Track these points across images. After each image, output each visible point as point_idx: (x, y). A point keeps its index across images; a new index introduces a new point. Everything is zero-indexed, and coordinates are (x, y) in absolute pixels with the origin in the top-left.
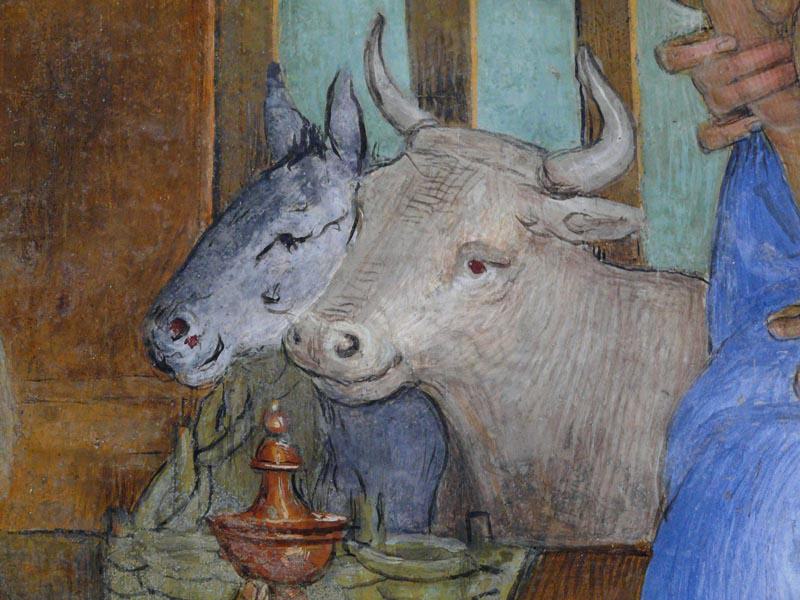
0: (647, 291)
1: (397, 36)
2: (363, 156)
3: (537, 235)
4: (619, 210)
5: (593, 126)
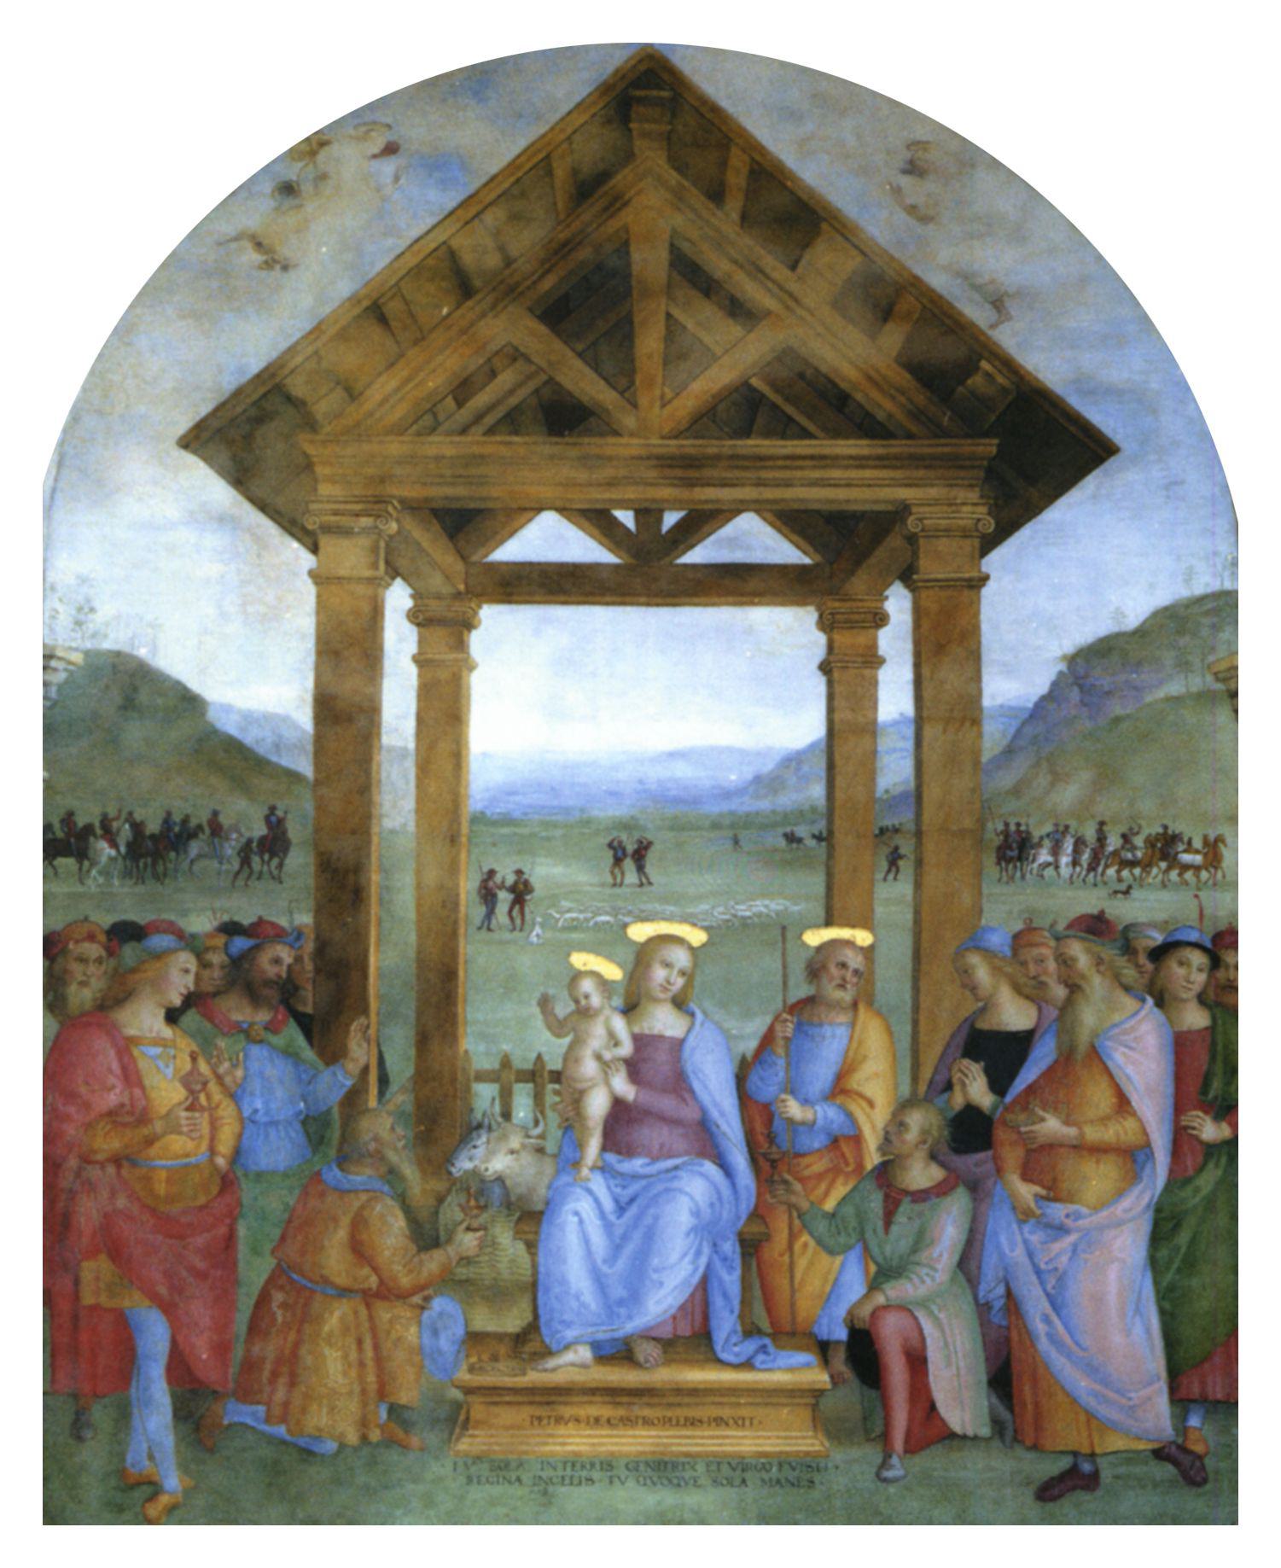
1: (497, 1102)
2: (490, 1129)
3: (524, 1146)
4: (539, 1141)
5: (536, 1123)
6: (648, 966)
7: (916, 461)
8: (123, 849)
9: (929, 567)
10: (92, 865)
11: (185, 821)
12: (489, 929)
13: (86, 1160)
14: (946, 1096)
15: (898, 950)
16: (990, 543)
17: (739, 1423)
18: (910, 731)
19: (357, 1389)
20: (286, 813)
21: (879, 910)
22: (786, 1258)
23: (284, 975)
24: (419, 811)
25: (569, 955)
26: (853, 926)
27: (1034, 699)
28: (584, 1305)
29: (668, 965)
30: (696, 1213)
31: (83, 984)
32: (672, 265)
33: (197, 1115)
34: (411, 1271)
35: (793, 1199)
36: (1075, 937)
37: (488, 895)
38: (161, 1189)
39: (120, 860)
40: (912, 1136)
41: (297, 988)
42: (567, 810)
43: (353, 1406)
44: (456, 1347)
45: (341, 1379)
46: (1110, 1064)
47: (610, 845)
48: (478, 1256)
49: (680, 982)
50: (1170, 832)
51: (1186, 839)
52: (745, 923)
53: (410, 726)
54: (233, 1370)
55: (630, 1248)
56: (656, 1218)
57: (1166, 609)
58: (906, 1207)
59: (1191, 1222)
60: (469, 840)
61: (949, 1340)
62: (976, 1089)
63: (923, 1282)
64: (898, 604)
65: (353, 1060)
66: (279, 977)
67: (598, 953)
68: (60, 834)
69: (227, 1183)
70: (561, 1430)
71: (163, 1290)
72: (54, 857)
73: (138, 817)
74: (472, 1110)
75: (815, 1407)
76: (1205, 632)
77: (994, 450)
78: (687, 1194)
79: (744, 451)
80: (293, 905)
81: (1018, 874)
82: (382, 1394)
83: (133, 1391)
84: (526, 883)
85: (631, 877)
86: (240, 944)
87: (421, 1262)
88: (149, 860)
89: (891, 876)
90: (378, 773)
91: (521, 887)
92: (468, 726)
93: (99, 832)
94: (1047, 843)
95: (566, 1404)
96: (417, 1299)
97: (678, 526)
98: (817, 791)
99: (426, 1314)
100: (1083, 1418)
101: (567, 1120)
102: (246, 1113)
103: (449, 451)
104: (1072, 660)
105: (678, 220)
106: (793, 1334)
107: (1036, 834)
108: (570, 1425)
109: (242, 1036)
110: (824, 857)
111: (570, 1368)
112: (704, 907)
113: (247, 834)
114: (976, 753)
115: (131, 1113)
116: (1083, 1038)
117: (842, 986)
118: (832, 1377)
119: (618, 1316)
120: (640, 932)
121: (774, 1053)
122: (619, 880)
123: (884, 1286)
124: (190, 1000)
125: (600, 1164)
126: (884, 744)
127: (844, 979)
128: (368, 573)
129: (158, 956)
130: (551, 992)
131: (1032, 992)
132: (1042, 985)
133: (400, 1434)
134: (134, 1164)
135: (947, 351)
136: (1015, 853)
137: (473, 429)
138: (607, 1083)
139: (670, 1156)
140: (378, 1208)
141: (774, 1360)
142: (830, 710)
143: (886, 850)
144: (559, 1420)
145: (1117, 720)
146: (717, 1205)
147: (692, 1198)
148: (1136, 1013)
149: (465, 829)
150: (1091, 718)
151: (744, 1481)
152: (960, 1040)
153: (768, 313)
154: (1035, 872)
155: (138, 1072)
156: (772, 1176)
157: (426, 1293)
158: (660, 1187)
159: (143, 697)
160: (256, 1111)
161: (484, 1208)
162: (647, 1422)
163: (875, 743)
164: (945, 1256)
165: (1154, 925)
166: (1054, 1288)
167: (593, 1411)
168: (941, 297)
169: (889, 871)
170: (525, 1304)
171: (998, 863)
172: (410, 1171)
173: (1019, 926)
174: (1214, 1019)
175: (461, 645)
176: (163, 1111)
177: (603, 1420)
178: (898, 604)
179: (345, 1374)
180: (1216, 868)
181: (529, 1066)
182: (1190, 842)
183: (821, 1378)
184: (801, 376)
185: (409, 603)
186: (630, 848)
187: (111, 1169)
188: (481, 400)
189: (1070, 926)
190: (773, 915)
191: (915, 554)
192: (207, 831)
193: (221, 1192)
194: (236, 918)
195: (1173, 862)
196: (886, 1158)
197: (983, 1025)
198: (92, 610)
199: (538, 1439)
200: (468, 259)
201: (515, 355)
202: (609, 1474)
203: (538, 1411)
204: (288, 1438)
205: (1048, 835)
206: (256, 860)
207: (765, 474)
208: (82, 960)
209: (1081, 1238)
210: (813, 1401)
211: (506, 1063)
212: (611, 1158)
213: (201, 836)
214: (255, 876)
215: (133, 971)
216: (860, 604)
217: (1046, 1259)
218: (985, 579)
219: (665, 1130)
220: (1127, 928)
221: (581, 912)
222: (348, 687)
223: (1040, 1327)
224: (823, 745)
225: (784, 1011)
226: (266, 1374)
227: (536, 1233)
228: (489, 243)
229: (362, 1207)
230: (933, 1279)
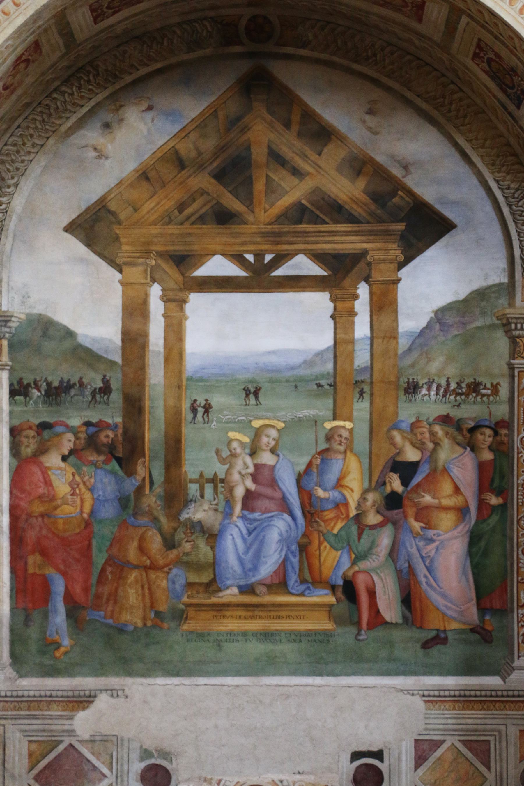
0: (219, 513)
1: (198, 492)
2: (195, 502)
3: (210, 508)
5: (215, 499)
6: (260, 436)
7: (371, 233)
8: (43, 393)
9: (376, 276)
10: (30, 399)
11: (69, 381)
12: (194, 423)
13: (30, 515)
14: (383, 487)
16: (401, 265)
17: (298, 618)
18: (369, 342)
19: (142, 605)
20: (110, 377)
21: (355, 414)
22: (318, 552)
23: (110, 442)
24: (165, 377)
25: (227, 433)
26: (345, 421)
27: (421, 328)
28: (235, 571)
29: (268, 436)
30: (280, 534)
31: (27, 446)
32: (269, 154)
33: (75, 497)
34: (163, 558)
35: (321, 529)
36: (437, 424)
37: (194, 410)
38: (61, 527)
39: (42, 397)
40: (369, 503)
42: (225, 375)
43: (140, 612)
44: (182, 588)
45: (135, 601)
46: (452, 474)
47: (244, 389)
48: (191, 552)
49: (273, 443)
50: (477, 381)
51: (484, 384)
52: (300, 420)
53: (161, 342)
54: (91, 597)
55: (252, 550)
56: (264, 537)
57: (476, 291)
58: (366, 532)
60: (186, 389)
61: (386, 585)
63: (374, 561)
65: (139, 475)
66: (108, 443)
67: (239, 432)
68: (17, 387)
69: (88, 524)
70: (225, 621)
71: (62, 567)
72: (15, 396)
73: (50, 379)
74: (188, 494)
75: (330, 611)
76: (492, 300)
77: (404, 227)
78: (277, 526)
79: (299, 230)
80: (114, 414)
81: (413, 399)
82: (152, 607)
83: (50, 607)
84: (209, 405)
85: (253, 401)
86: (92, 430)
87: (168, 555)
88: (54, 397)
89: (360, 400)
90: (148, 361)
91: (207, 406)
92: (185, 341)
93: (33, 386)
94: (425, 386)
95: (227, 610)
96: (166, 569)
97: (272, 260)
98: (329, 367)
99: (170, 575)
100: (441, 615)
101: (227, 498)
102: (95, 496)
103: (176, 232)
104: (436, 312)
105: (272, 136)
106: (320, 582)
107: (421, 383)
108: (229, 619)
109: (93, 466)
110: (332, 393)
111: (230, 596)
112: (283, 413)
113: (94, 386)
114: (396, 350)
115: (48, 497)
116: (440, 464)
117: (340, 444)
118: (337, 599)
119: (249, 576)
120: (256, 424)
121: (311, 470)
122: (248, 403)
123: (358, 563)
125: (241, 515)
126: (357, 347)
127: (341, 441)
128: (143, 281)
129: (59, 435)
130: (220, 447)
131: (420, 446)
132: (423, 443)
133: (160, 623)
136: (412, 390)
137: (185, 223)
138: (244, 484)
139: (269, 512)
140: (150, 533)
141: (313, 592)
142: (335, 334)
143: (358, 390)
144: (224, 617)
145: (456, 336)
146: (289, 531)
147: (279, 528)
148: (463, 454)
149: (184, 383)
150: (444, 335)
151: (300, 641)
152: (389, 465)
153: (309, 174)
154: (420, 398)
155: (50, 480)
156: (311, 519)
157: (170, 567)
158: (266, 524)
159: (51, 332)
160: (99, 495)
161: (192, 533)
162: (261, 618)
163: (354, 347)
164: (383, 551)
165: (470, 419)
166: (429, 563)
167: (239, 613)
168: (381, 165)
169: (359, 399)
170: (211, 570)
171: (405, 395)
172: (163, 519)
173: (413, 420)
174: (495, 455)
175: (182, 309)
176: (61, 496)
177: (243, 617)
179: (137, 599)
180: (496, 396)
181: (212, 477)
182: (485, 385)
183: (332, 600)
184: (323, 199)
185: (161, 293)
186: (252, 390)
187: (40, 519)
188: (189, 211)
189: (434, 420)
190: (312, 416)
191: (370, 270)
192: (78, 385)
193: (85, 528)
194: (90, 420)
195: (478, 393)
196: (359, 512)
197: (399, 459)
198: (29, 297)
199: (216, 624)
200: (183, 153)
201: (203, 192)
202: (245, 638)
203: (215, 613)
204: (113, 624)
205: (426, 383)
206: (98, 397)
207: (307, 239)
208: (27, 437)
209: (440, 544)
210: (328, 609)
211: (201, 475)
212: (246, 513)
213: (75, 387)
214: (98, 403)
215: (49, 441)
216: (346, 291)
217: (426, 552)
218: (400, 280)
219: (267, 501)
220: (459, 420)
221: (232, 416)
222: (135, 327)
223: (423, 580)
224: (332, 348)
225: (316, 454)
226: (104, 599)
227: (215, 543)
228: (191, 146)
229: (144, 533)
230: (378, 560)
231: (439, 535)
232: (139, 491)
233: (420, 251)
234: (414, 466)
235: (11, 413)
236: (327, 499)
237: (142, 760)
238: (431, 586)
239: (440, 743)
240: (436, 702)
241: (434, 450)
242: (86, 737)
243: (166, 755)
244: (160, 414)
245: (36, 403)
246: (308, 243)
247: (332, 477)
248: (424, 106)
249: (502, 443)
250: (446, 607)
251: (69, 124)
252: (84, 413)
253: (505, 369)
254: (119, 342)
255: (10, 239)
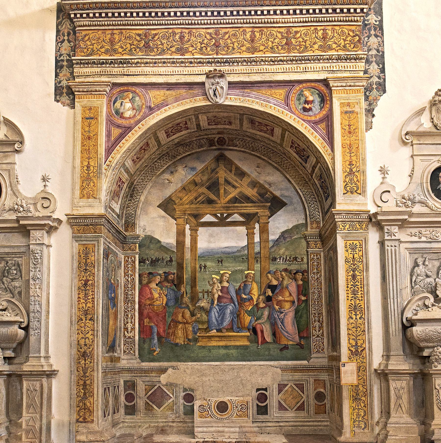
7: (259, 206)
9: (261, 221)
15: (258, 274)
16: (269, 217)
17: (237, 340)
21: (255, 268)
30: (230, 311)
37: (201, 268)
38: (156, 309)
40: (261, 300)
41: (174, 281)
43: (183, 339)
59: (301, 311)
62: (269, 293)
64: (257, 226)
71: (156, 323)
98: (246, 252)
120: (222, 272)
124: (159, 283)
129: (155, 276)
131: (277, 279)
132: (278, 278)
134: (151, 305)
135: (263, 191)
142: (248, 241)
145: (289, 241)
162: (224, 341)
167: (216, 339)
175: (196, 233)
178: (257, 226)
188: (198, 200)
195: (297, 261)
197: (270, 284)
201: (203, 194)
208: (145, 277)
222: (181, 239)
231: (285, 311)
232: (182, 295)
233: (276, 213)
234: (276, 286)
235: (139, 269)
236: (246, 298)
237: (184, 392)
238: (283, 329)
239: (286, 385)
240: (285, 370)
241: (282, 281)
242: (165, 384)
243: (192, 390)
244: (189, 269)
245: (148, 265)
246: (238, 210)
247: (247, 291)
248: (276, 165)
249: (305, 278)
250: (288, 336)
251: (160, 172)
252: (164, 269)
253: (305, 252)
254: (175, 245)
255: (140, 210)
